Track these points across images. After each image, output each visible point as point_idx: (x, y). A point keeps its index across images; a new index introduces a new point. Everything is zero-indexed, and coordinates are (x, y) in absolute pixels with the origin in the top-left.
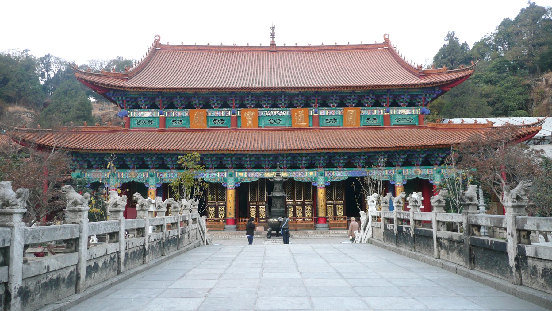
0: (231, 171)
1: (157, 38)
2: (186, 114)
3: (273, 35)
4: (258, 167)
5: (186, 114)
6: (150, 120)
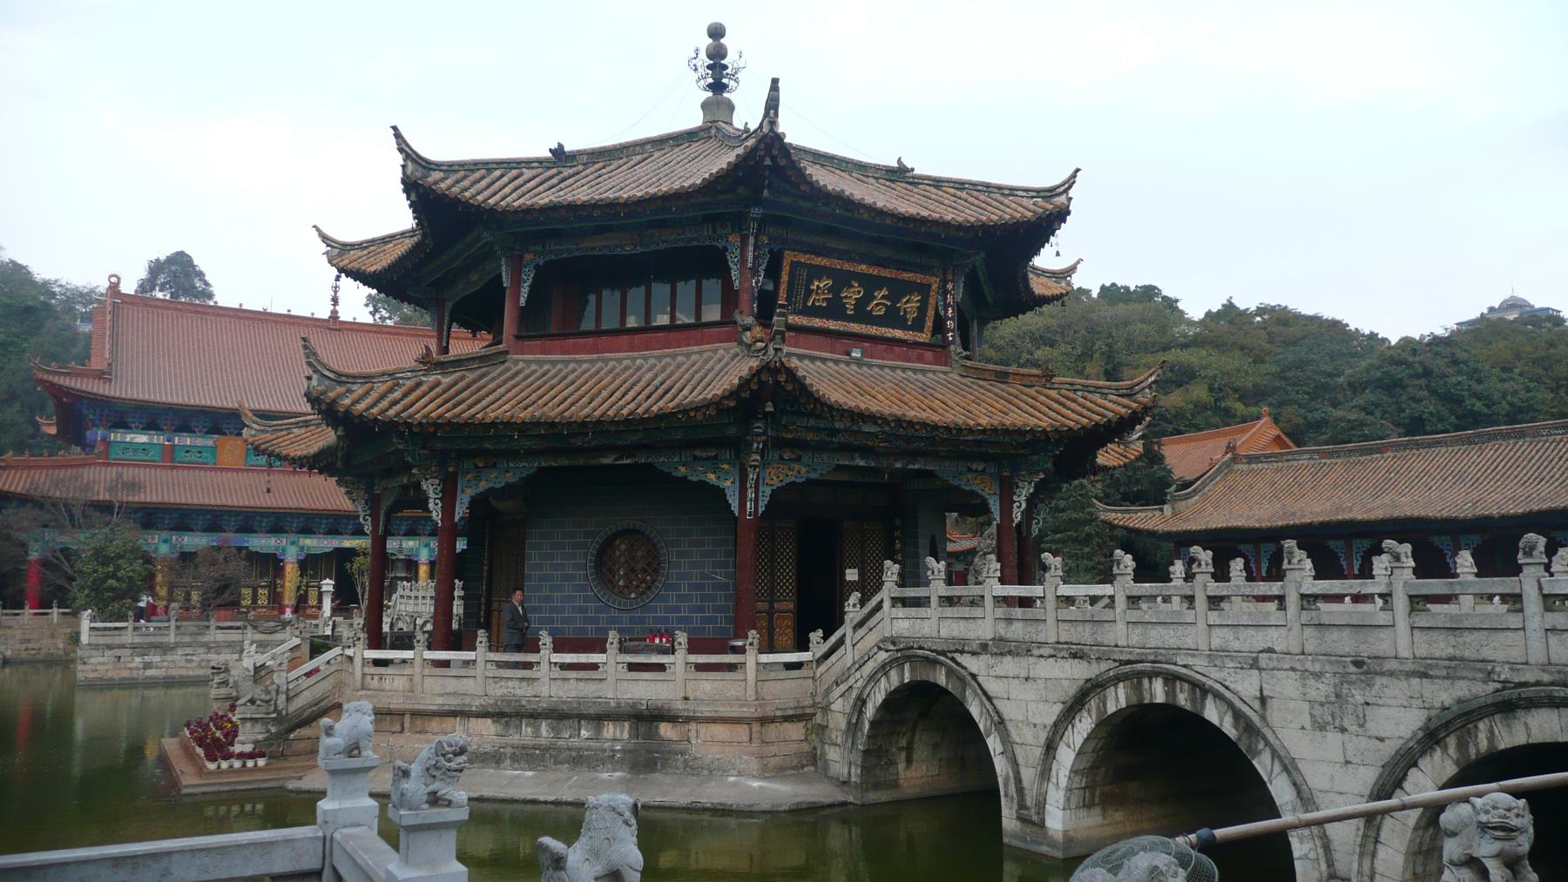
0: (293, 537)
1: (114, 280)
2: (210, 443)
3: (335, 301)
4: (333, 531)
5: (210, 443)
6: (145, 448)
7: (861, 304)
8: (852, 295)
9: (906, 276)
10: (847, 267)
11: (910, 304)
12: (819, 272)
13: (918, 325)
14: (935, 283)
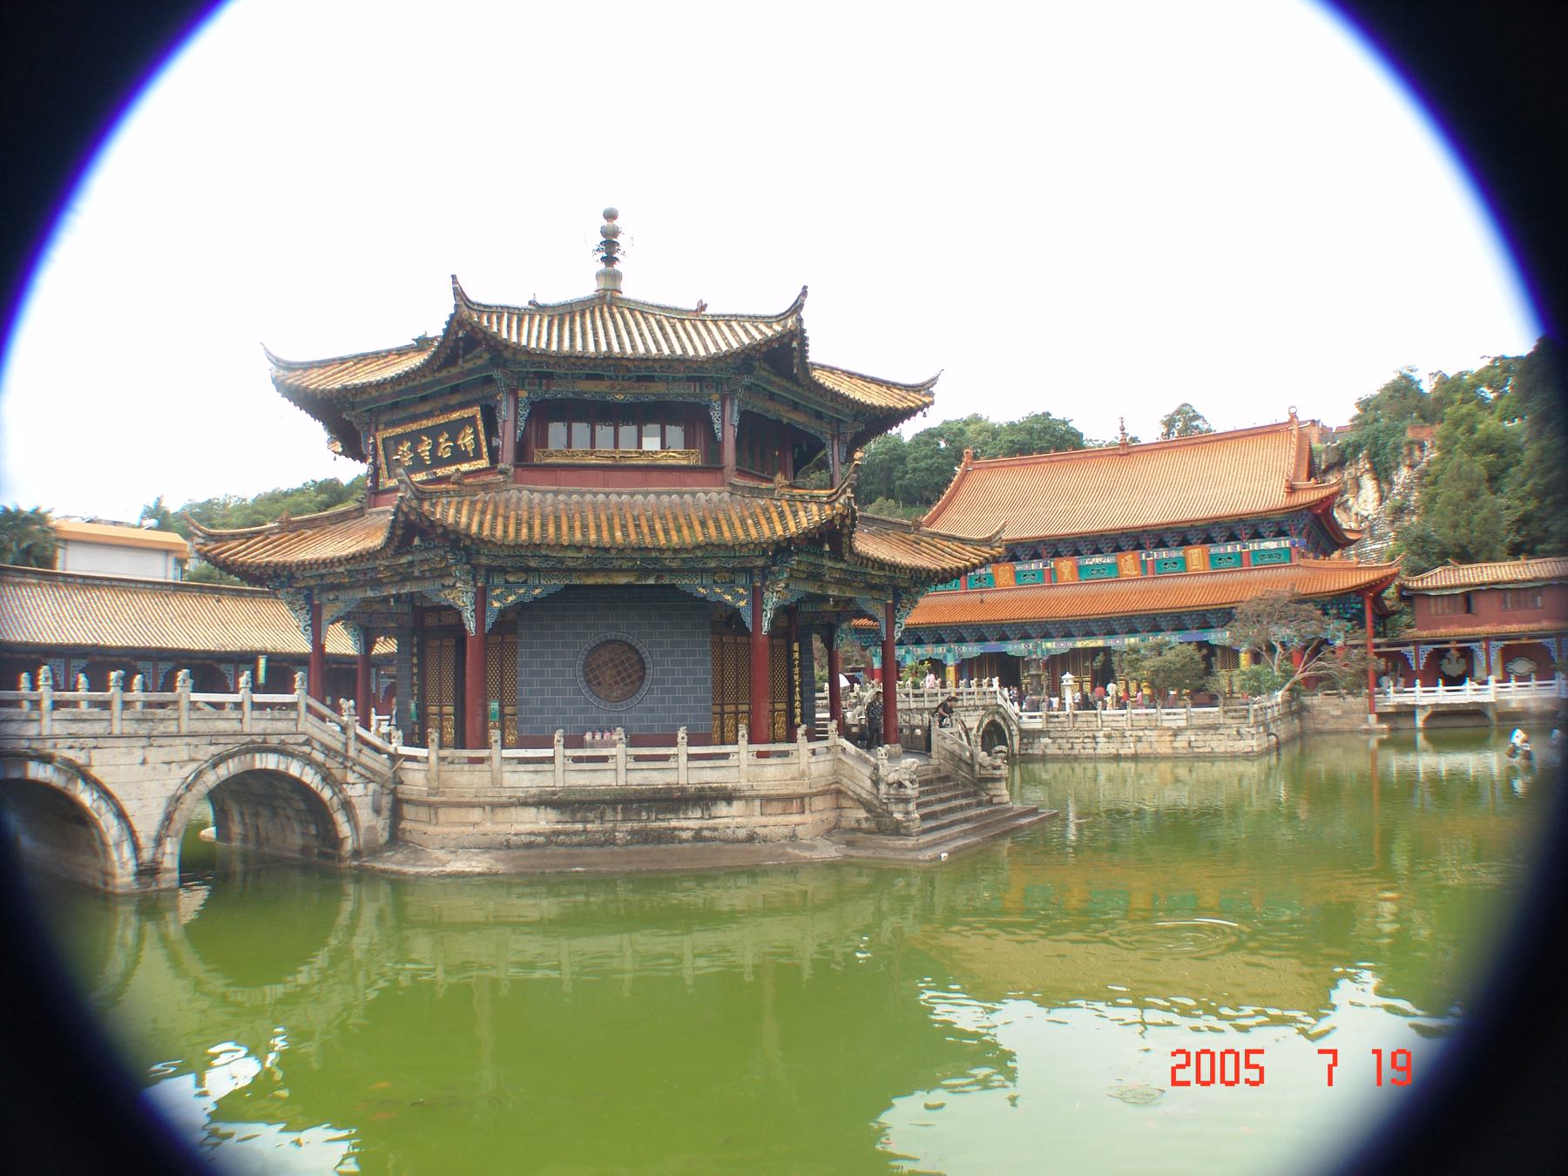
7: (433, 452)
8: (425, 448)
9: (455, 416)
10: (414, 427)
11: (466, 440)
12: (399, 440)
13: (478, 455)
14: (475, 411)
